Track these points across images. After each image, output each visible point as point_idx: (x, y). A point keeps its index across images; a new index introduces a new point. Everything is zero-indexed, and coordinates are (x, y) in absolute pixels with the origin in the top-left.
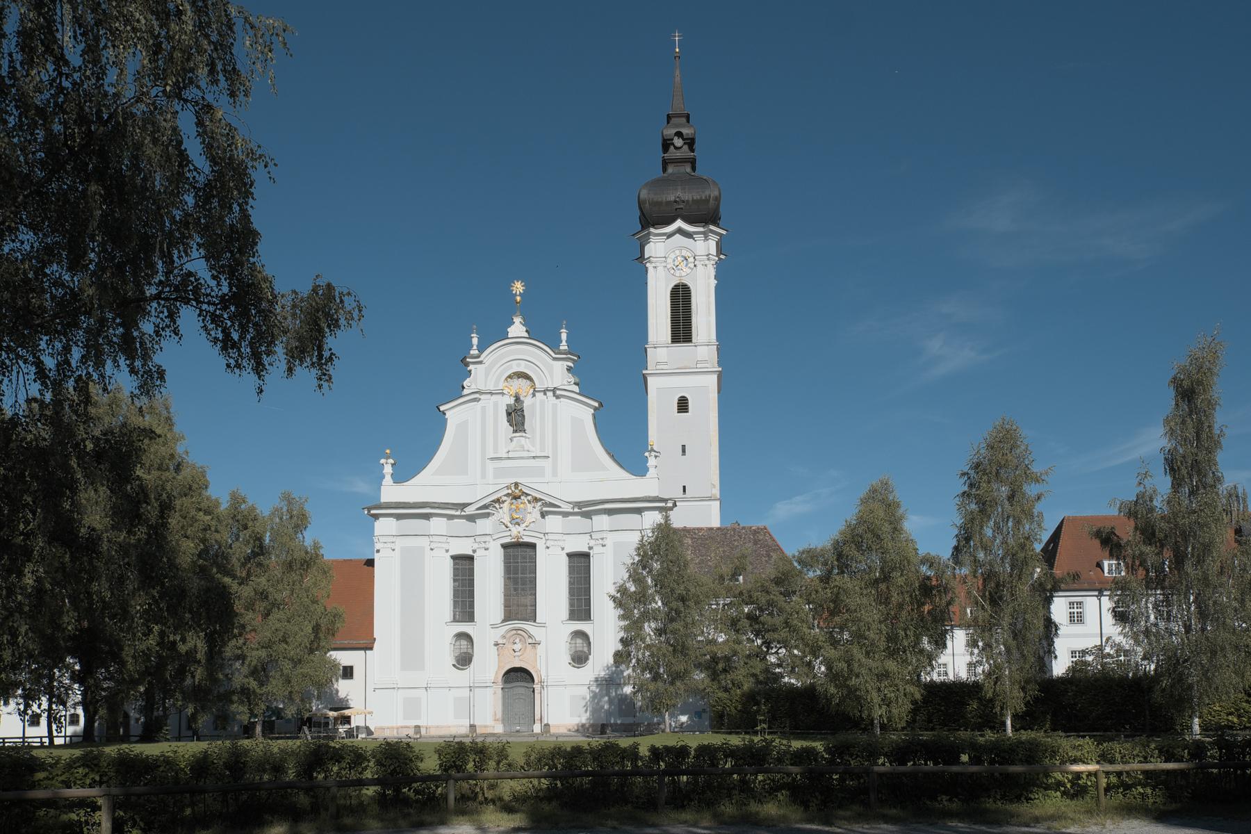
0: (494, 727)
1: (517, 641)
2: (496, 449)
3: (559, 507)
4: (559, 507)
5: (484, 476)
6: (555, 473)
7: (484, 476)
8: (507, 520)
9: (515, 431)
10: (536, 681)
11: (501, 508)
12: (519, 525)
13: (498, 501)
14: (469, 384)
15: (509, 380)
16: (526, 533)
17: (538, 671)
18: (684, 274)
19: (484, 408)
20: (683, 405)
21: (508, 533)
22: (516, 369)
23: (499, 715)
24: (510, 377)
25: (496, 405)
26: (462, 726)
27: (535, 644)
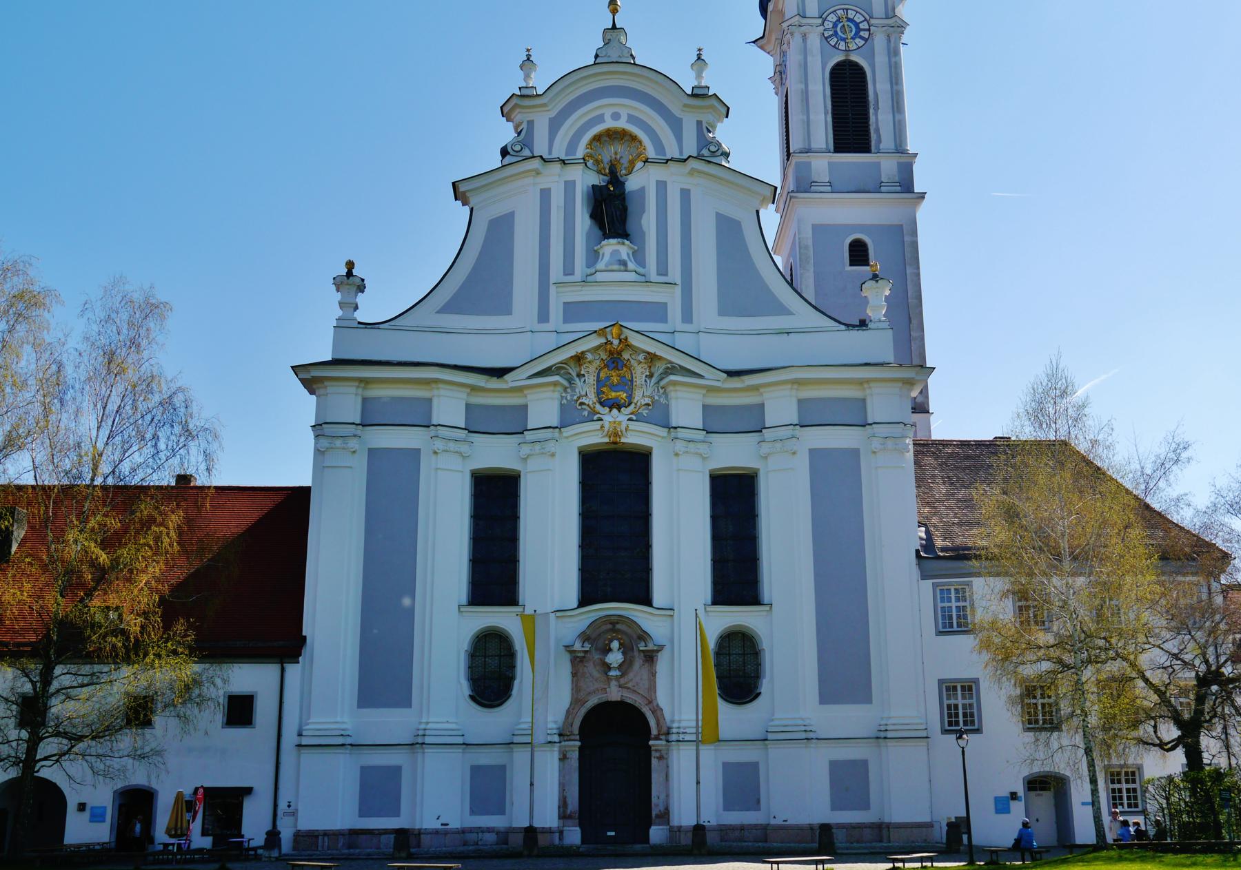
0: (561, 833)
1: (615, 645)
2: (569, 270)
3: (700, 376)
4: (700, 376)
5: (543, 316)
6: (687, 317)
7: (543, 316)
8: (591, 399)
9: (606, 236)
10: (654, 732)
11: (579, 375)
12: (619, 411)
13: (579, 359)
14: (518, 148)
15: (595, 143)
16: (633, 425)
17: (657, 711)
18: (852, 46)
19: (545, 194)
20: (858, 253)
21: (597, 425)
22: (609, 124)
23: (573, 803)
24: (597, 138)
25: (570, 186)
26: (490, 830)
27: (650, 658)
